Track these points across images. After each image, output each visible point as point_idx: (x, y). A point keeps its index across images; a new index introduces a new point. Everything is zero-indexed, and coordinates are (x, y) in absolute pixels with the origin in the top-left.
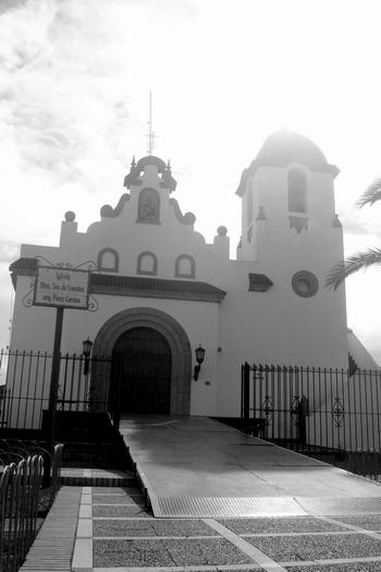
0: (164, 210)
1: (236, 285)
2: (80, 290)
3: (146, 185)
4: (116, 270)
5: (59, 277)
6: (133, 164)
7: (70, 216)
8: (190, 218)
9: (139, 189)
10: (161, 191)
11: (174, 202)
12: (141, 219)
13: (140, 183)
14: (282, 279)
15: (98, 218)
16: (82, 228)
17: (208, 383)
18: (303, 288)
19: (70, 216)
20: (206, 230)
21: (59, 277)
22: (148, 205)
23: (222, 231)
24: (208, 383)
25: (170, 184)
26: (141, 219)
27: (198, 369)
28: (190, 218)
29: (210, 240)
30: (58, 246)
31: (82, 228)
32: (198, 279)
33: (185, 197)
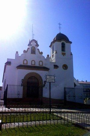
0: (37, 51)
1: (51, 67)
2: (53, 79)
3: (32, 46)
4: (27, 64)
5: (50, 77)
6: (30, 41)
7: (17, 52)
8: (42, 53)
9: (31, 46)
10: (36, 47)
11: (38, 49)
12: (32, 53)
13: (31, 45)
14: (60, 65)
15: (23, 53)
16: (20, 55)
17: (46, 88)
18: (64, 68)
19: (17, 52)
20: (45, 55)
21: (50, 77)
22: (33, 50)
23: (48, 56)
24: (46, 88)
25: (37, 45)
26: (32, 53)
27: (44, 85)
28: (42, 53)
29: (46, 58)
30: (14, 58)
31: (20, 55)
32: (44, 66)
33: (41, 48)
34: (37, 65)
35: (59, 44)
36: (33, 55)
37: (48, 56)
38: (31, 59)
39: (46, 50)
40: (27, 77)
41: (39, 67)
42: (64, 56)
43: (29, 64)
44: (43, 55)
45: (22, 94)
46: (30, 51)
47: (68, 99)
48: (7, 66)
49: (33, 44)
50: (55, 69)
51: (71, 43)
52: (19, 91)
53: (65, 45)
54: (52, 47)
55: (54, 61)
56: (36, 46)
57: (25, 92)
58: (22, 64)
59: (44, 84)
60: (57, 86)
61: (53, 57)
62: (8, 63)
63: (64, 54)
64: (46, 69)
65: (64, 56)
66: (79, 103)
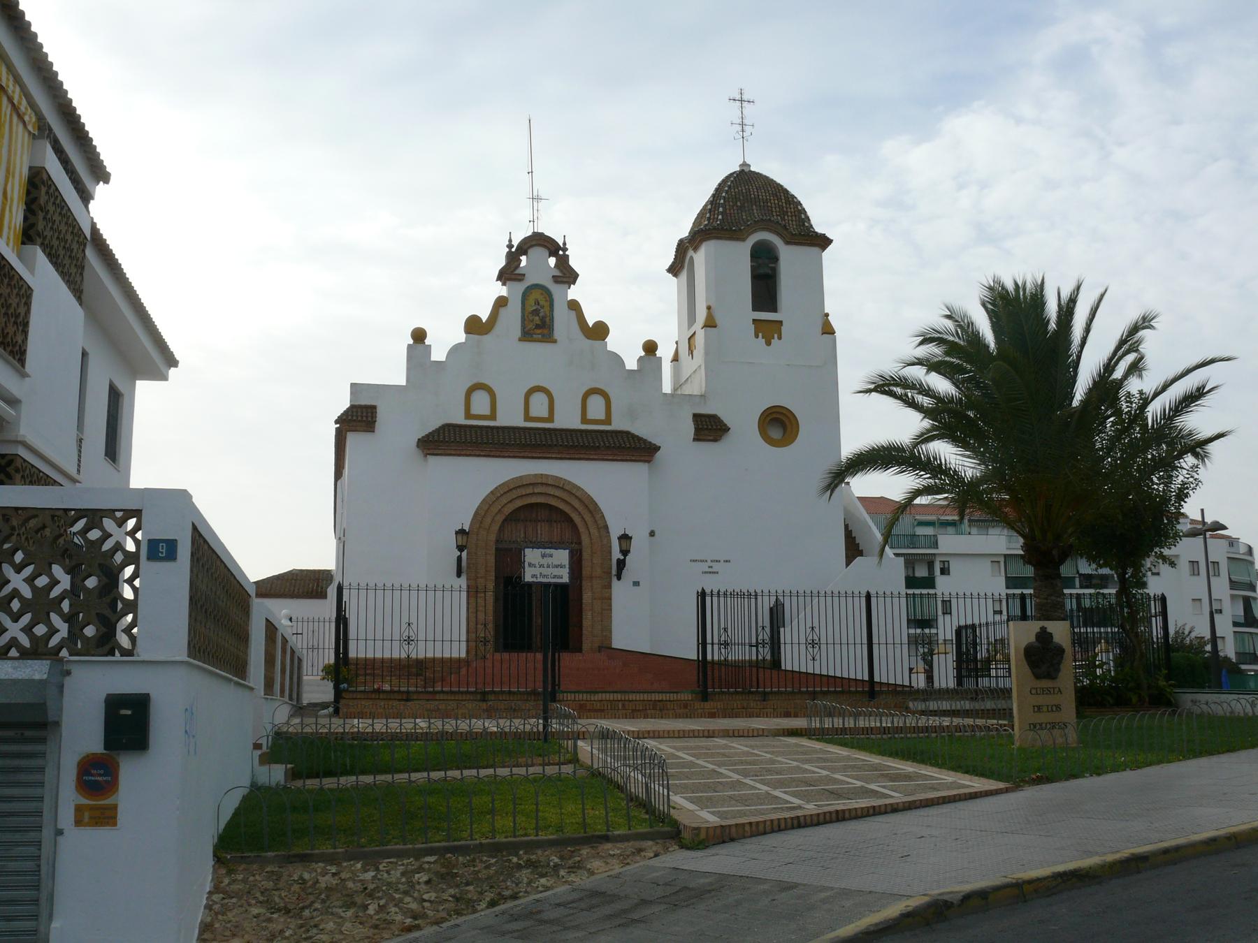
0: (561, 317)
1: (674, 436)
2: (561, 566)
3: (531, 280)
4: (493, 416)
5: (543, 556)
6: (510, 246)
7: (419, 336)
8: (600, 331)
9: (520, 287)
10: (555, 289)
11: (574, 306)
12: (527, 336)
13: (520, 278)
14: (743, 421)
15: (461, 337)
16: (439, 354)
17: (636, 584)
18: (776, 433)
19: (419, 336)
20: (625, 346)
21: (543, 556)
22: (536, 312)
23: (650, 348)
24: (636, 584)
25: (568, 276)
26: (527, 336)
27: (621, 564)
28: (600, 331)
29: (631, 364)
30: (401, 380)
31: (439, 354)
32: (618, 424)
33: (592, 295)
34: (568, 419)
35: (738, 256)
36: (537, 350)
37: (650, 348)
38: (524, 385)
39: (635, 298)
40: (495, 509)
41: (581, 431)
42: (768, 343)
43: (511, 416)
44: (612, 343)
45: (464, 638)
46: (512, 318)
47: (794, 659)
48: (352, 439)
49: (540, 267)
50: (707, 448)
51: (823, 242)
52: (413, 620)
53: (776, 259)
54: (684, 275)
55: (696, 387)
56: (556, 280)
57: (481, 616)
58: (460, 419)
59: (616, 555)
60: (716, 567)
61: (691, 352)
62: (358, 419)
63: (768, 331)
64: (633, 449)
65: (768, 343)
66: (888, 684)
